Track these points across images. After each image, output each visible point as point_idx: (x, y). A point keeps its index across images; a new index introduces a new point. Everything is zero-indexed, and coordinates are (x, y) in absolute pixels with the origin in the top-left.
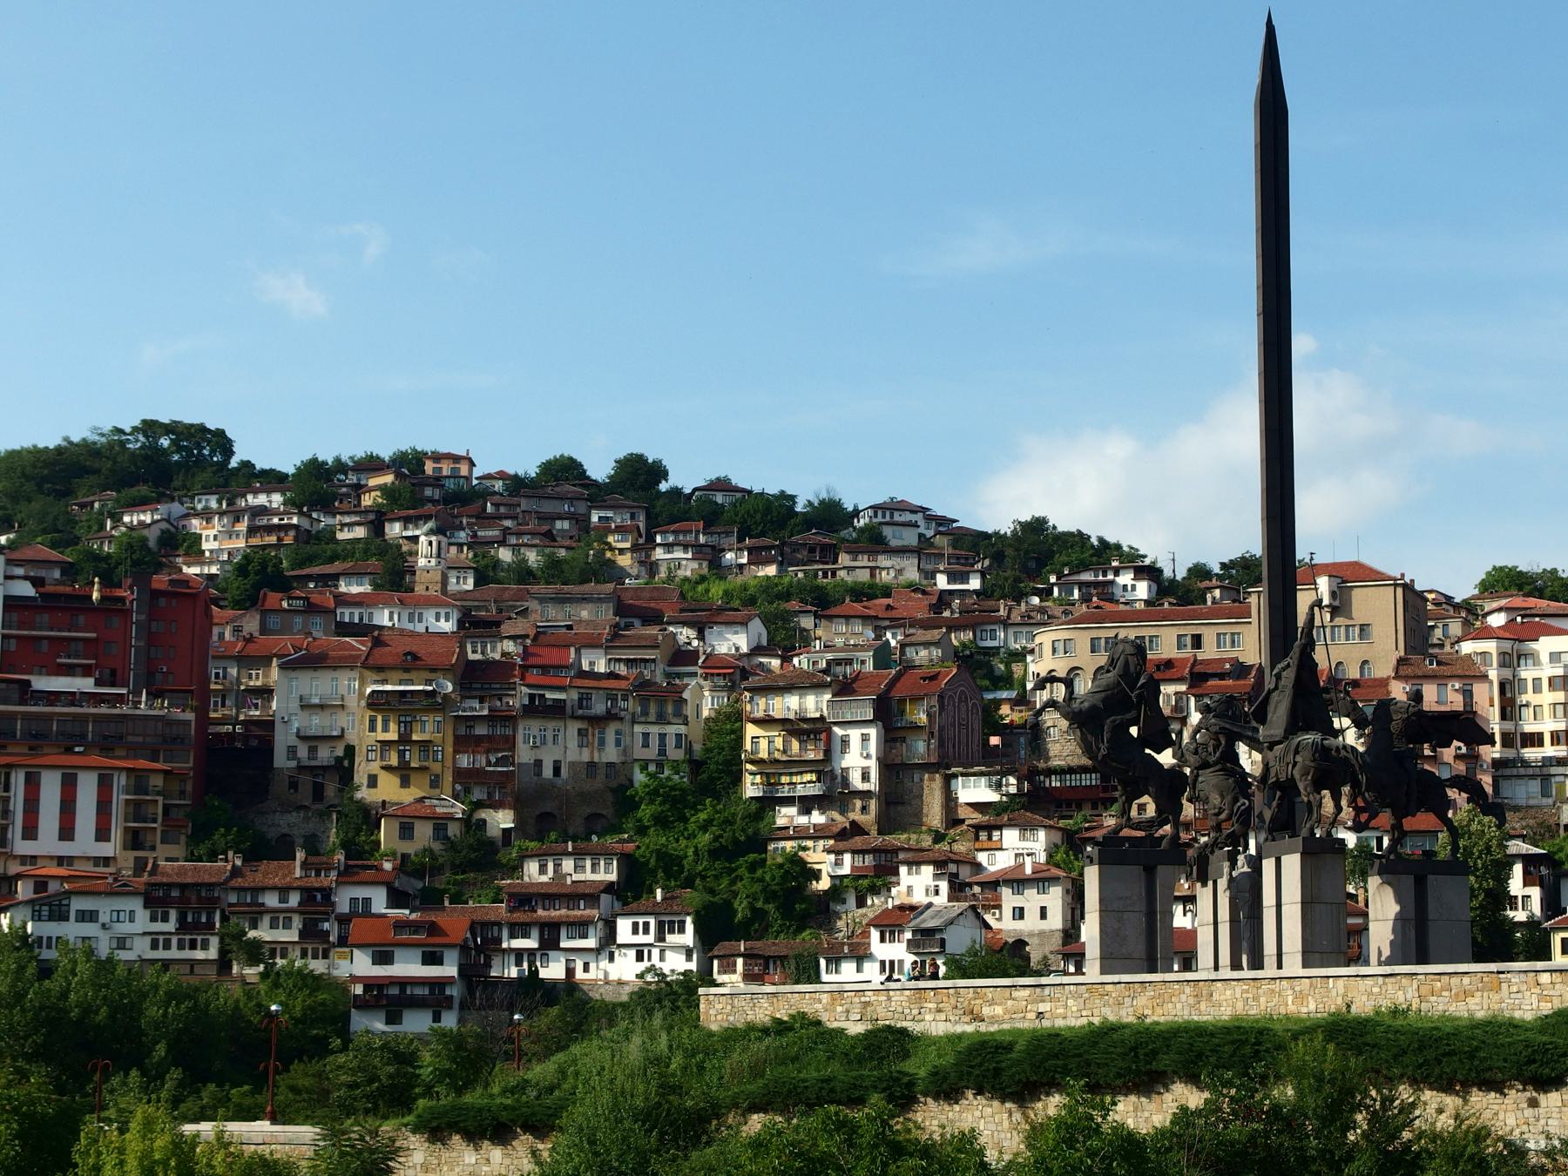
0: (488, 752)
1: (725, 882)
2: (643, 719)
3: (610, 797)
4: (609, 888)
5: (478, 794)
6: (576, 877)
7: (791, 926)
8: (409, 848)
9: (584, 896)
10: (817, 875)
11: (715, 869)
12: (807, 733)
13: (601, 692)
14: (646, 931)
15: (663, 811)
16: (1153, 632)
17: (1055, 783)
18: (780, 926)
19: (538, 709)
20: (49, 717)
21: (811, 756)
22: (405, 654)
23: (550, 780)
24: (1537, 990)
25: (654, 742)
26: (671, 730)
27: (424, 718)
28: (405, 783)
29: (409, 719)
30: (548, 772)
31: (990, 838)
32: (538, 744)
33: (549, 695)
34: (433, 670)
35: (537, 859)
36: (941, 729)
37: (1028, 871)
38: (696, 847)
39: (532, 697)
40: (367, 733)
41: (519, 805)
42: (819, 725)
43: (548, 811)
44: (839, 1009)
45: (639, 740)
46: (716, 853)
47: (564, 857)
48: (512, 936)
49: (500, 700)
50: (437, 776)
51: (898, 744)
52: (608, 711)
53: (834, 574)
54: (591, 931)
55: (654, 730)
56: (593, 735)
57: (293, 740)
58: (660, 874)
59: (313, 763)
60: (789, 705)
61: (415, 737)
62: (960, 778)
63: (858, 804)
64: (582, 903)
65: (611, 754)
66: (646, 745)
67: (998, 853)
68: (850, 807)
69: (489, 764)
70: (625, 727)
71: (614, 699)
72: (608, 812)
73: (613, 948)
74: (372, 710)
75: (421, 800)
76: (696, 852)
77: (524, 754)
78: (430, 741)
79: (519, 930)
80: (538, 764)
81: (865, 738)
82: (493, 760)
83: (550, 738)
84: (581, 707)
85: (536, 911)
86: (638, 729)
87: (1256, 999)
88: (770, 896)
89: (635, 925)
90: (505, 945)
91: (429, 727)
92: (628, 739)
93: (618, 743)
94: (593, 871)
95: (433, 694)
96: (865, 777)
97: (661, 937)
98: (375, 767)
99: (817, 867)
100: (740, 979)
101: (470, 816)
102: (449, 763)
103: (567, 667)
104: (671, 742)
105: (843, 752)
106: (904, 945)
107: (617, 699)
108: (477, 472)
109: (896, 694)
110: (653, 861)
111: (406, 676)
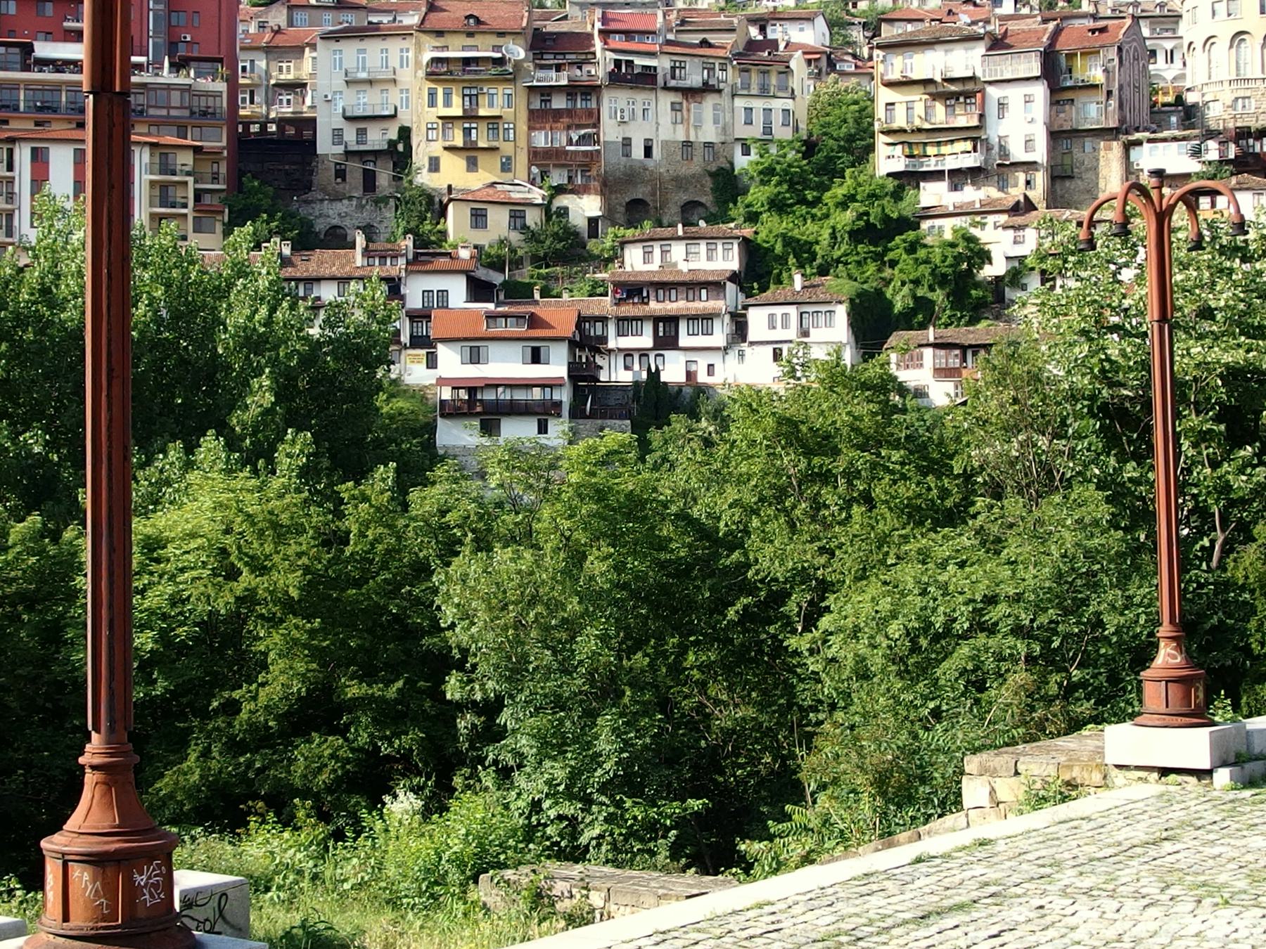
0: (569, 128)
1: (871, 268)
2: (745, 92)
3: (708, 183)
4: (734, 277)
5: (558, 177)
7: (962, 317)
8: (485, 238)
9: (706, 285)
10: (985, 257)
11: (858, 254)
12: (955, 96)
13: (696, 60)
14: (785, 325)
15: (779, 193)
18: (949, 317)
19: (625, 77)
20: (56, 87)
21: (961, 121)
22: (468, 17)
23: (640, 161)
25: (758, 118)
26: (778, 105)
27: (492, 91)
28: (472, 165)
29: (474, 92)
30: (638, 152)
31: (1213, 205)
32: (626, 119)
33: (638, 61)
34: (501, 34)
35: (640, 245)
36: (1121, 88)
38: (834, 228)
39: (618, 63)
40: (427, 109)
41: (607, 187)
42: (970, 87)
43: (640, 196)
45: (741, 116)
46: (856, 236)
47: (673, 243)
48: (620, 334)
49: (580, 68)
50: (509, 158)
51: (1067, 107)
52: (705, 83)
54: (717, 324)
55: (758, 104)
56: (688, 110)
57: (339, 122)
58: (792, 260)
59: (362, 148)
60: (927, 64)
61: (482, 112)
62: (1145, 145)
63: (1021, 177)
64: (704, 292)
65: (709, 133)
66: (749, 122)
68: (1011, 181)
69: (570, 142)
70: (724, 100)
71: (711, 70)
72: (707, 199)
73: (744, 346)
74: (433, 81)
75: (493, 184)
76: (833, 235)
77: (610, 131)
78: (500, 117)
80: (627, 142)
81: (1028, 100)
82: (575, 138)
83: (639, 113)
84: (673, 77)
85: (647, 304)
86: (740, 103)
88: (940, 280)
89: (772, 317)
90: (611, 344)
91: (499, 100)
92: (728, 116)
93: (716, 121)
94: (709, 258)
95: (500, 62)
96: (1029, 143)
98: (436, 149)
99: (987, 247)
101: (550, 202)
102: (522, 143)
103: (654, 33)
104: (777, 119)
105: (1001, 117)
107: (714, 69)
109: (1063, 45)
110: (779, 248)
111: (470, 41)
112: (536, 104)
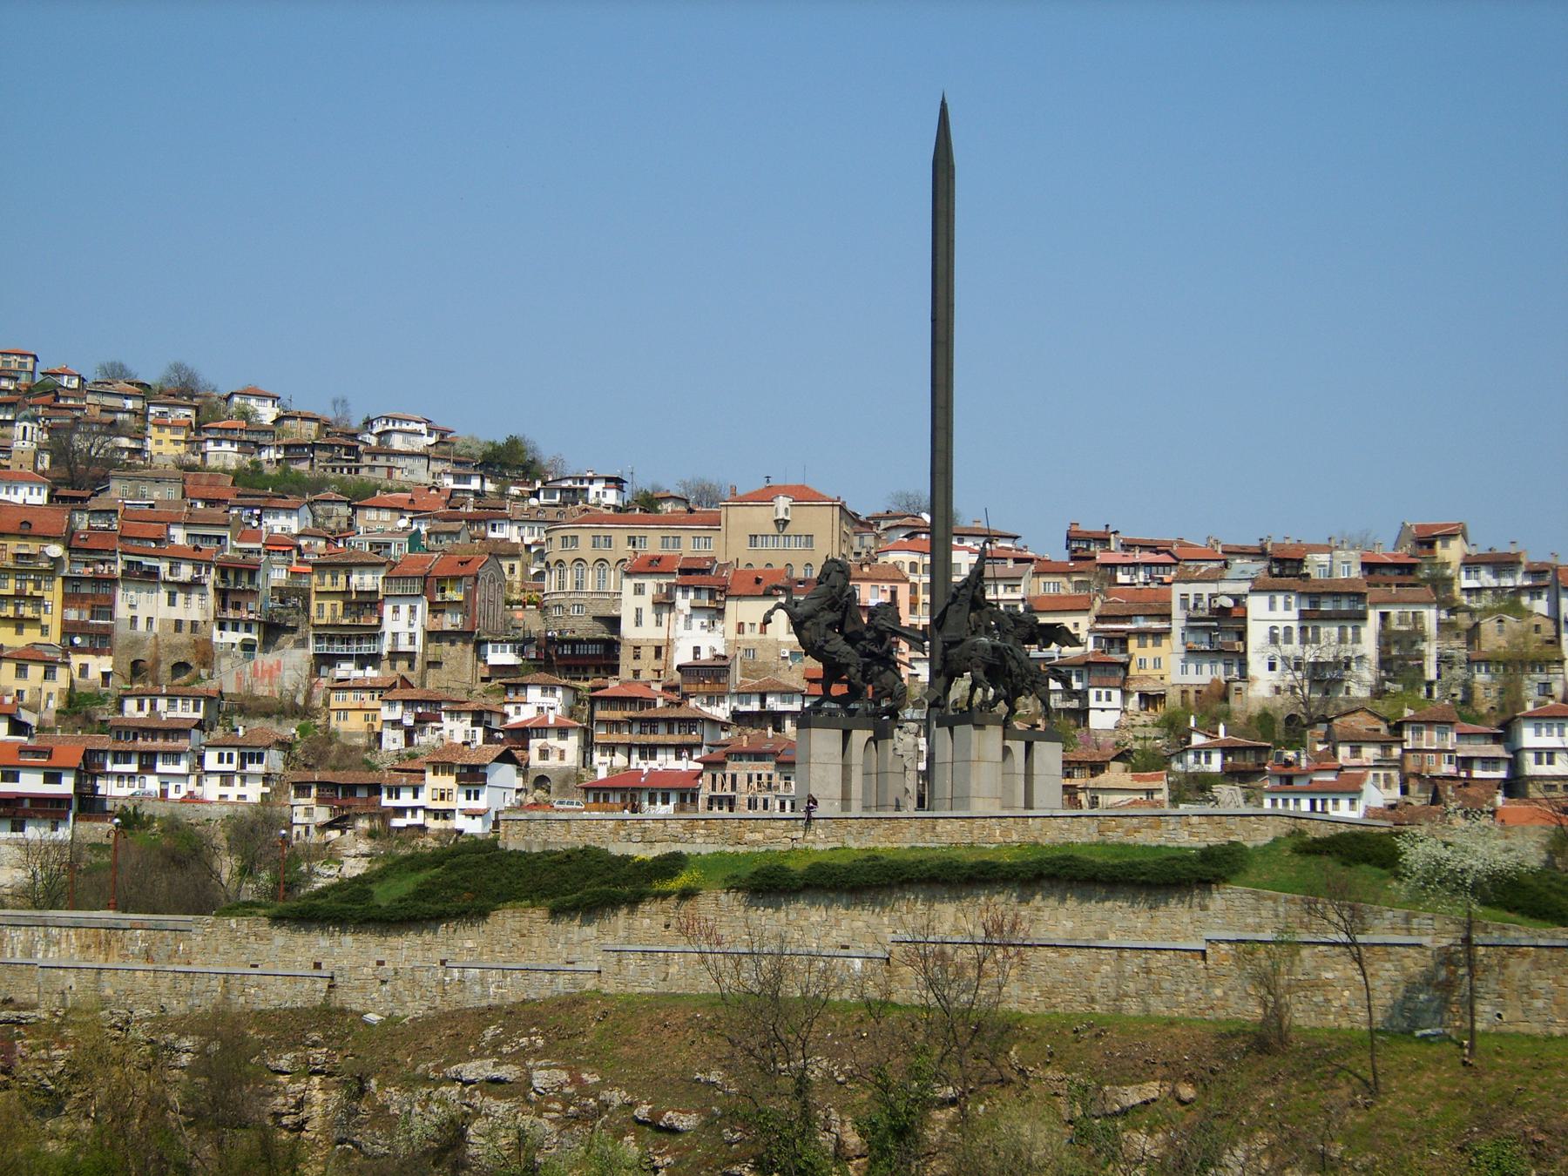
6: (171, 714)
14: (230, 761)
16: (642, 533)
17: (567, 651)
24: (1188, 828)
30: (142, 625)
37: (551, 721)
42: (373, 599)
44: (622, 833)
48: (115, 762)
53: (357, 471)
62: (490, 646)
67: (522, 706)
77: (122, 611)
79: (125, 757)
80: (134, 619)
87: (971, 832)
97: (243, 766)
100: (314, 801)
106: (454, 778)
108: (41, 368)
112: (70, 590)
